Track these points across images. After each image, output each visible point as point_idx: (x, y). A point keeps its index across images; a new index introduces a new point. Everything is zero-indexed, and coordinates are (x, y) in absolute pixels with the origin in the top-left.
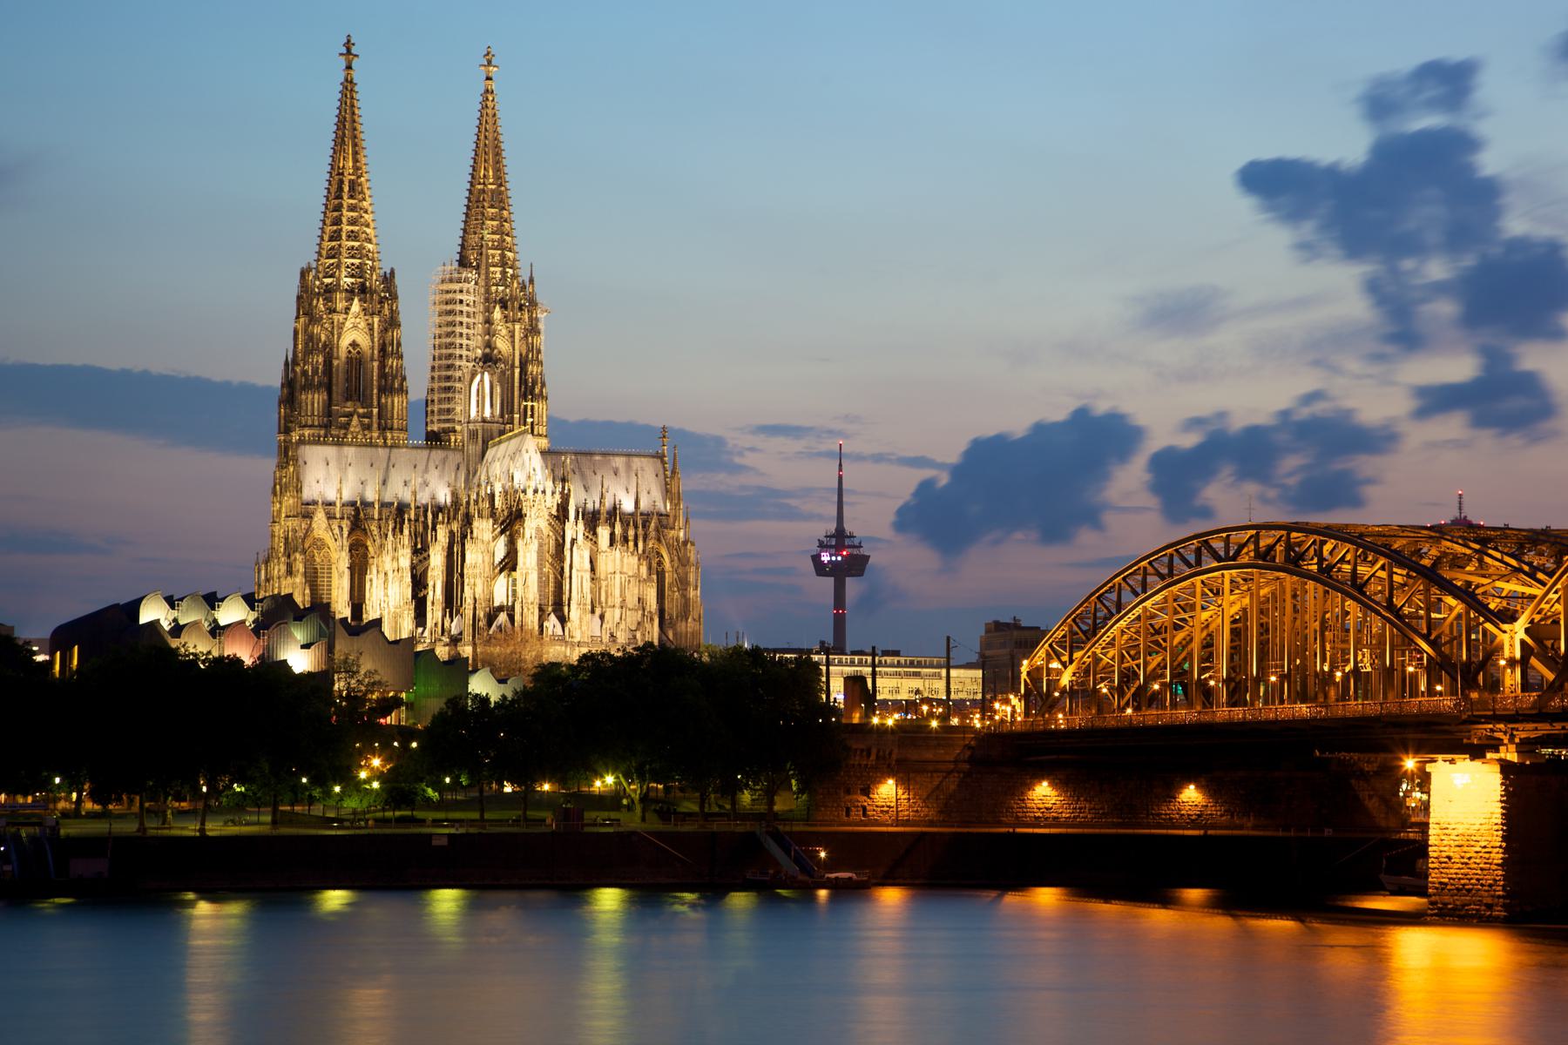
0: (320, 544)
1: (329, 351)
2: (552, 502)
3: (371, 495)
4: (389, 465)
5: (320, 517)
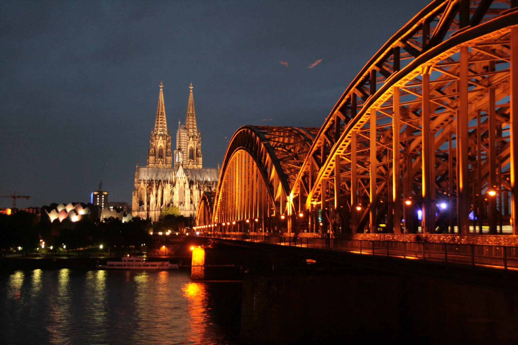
0: (142, 189)
2: (184, 180)
3: (154, 179)
5: (142, 183)
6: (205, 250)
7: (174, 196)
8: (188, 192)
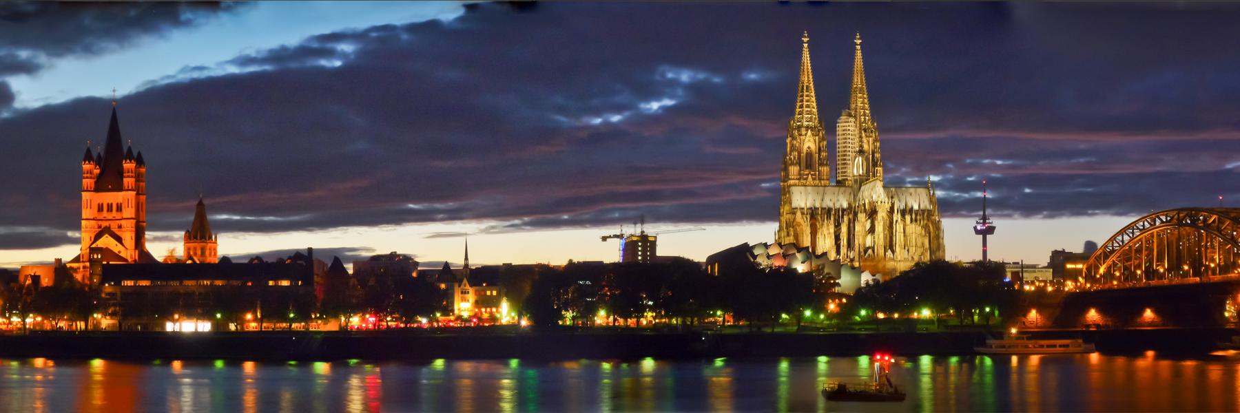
0: (799, 225)
2: (888, 206)
3: (818, 205)
4: (824, 193)
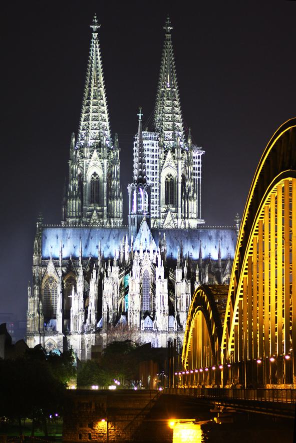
0: (51, 279)
1: (81, 178)
2: (152, 256)
3: (78, 254)
4: (89, 237)
5: (51, 267)
6: (203, 428)
7: (129, 297)
8: (162, 287)
